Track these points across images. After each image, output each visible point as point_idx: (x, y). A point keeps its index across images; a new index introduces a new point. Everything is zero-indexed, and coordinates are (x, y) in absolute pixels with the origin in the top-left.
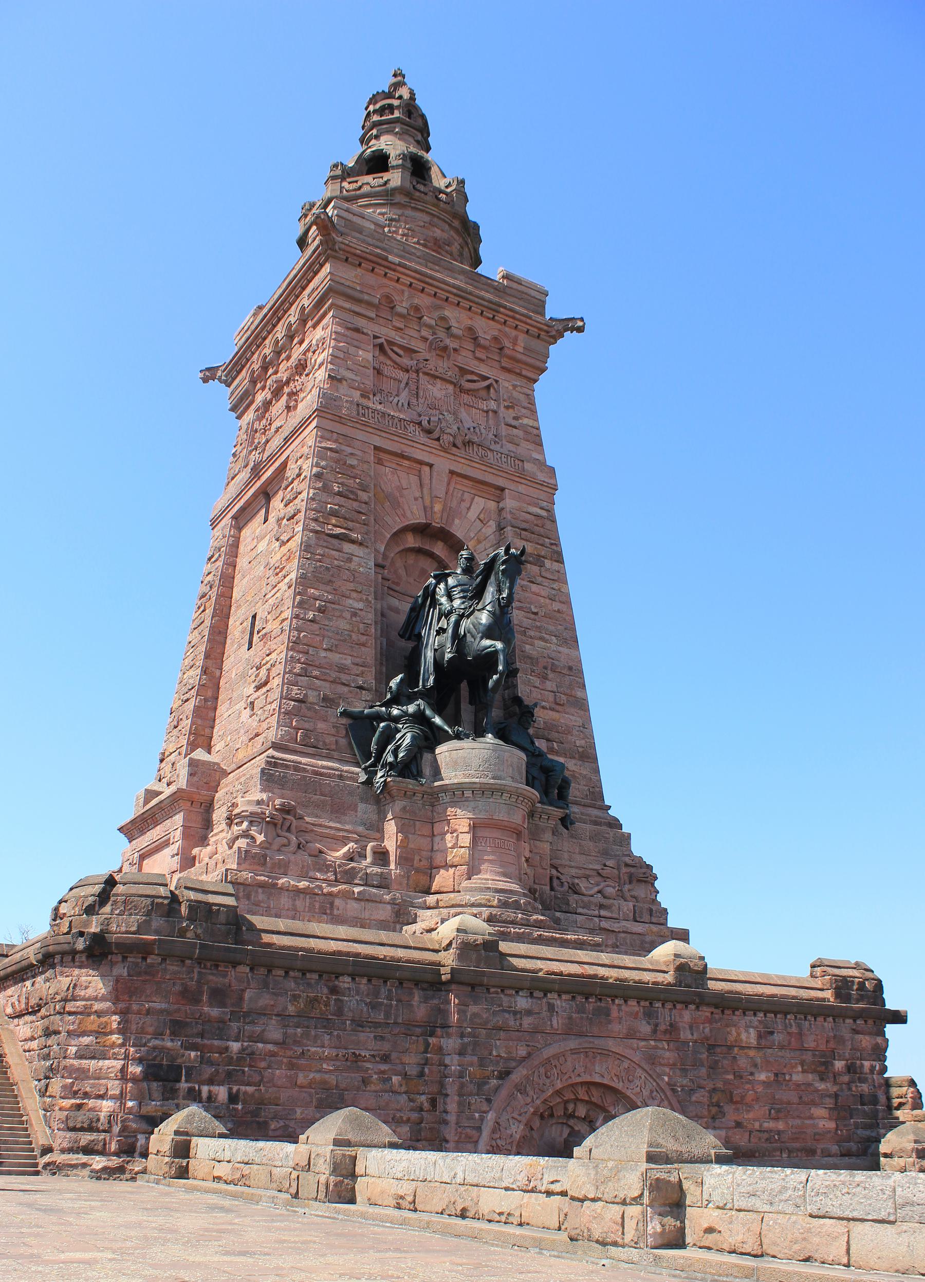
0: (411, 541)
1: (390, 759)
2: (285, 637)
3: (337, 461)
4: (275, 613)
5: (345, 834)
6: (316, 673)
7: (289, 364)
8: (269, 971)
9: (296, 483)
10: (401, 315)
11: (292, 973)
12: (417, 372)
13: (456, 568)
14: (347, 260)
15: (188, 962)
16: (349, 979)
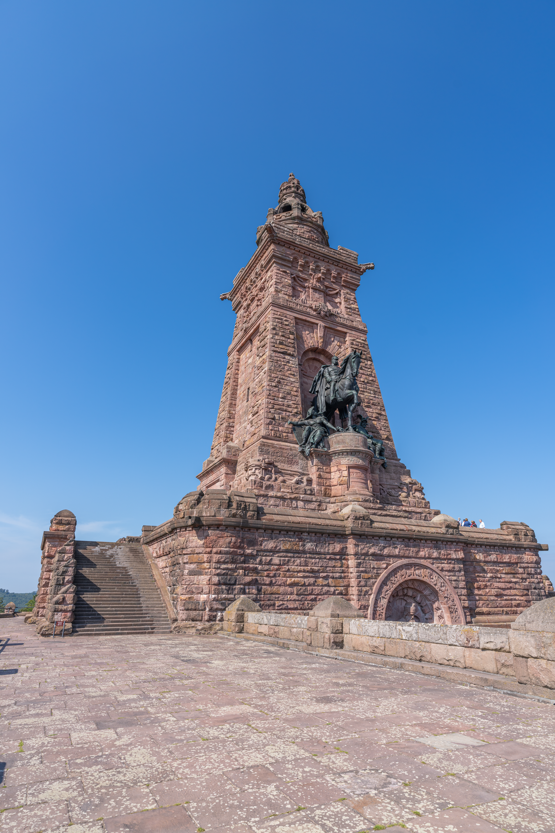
0: (311, 355)
1: (312, 441)
2: (264, 393)
3: (281, 323)
4: (259, 385)
5: (294, 473)
7: (257, 288)
8: (272, 531)
9: (264, 333)
11: (282, 532)
12: (309, 288)
13: (331, 363)
14: (279, 244)
15: (237, 529)
16: (306, 534)
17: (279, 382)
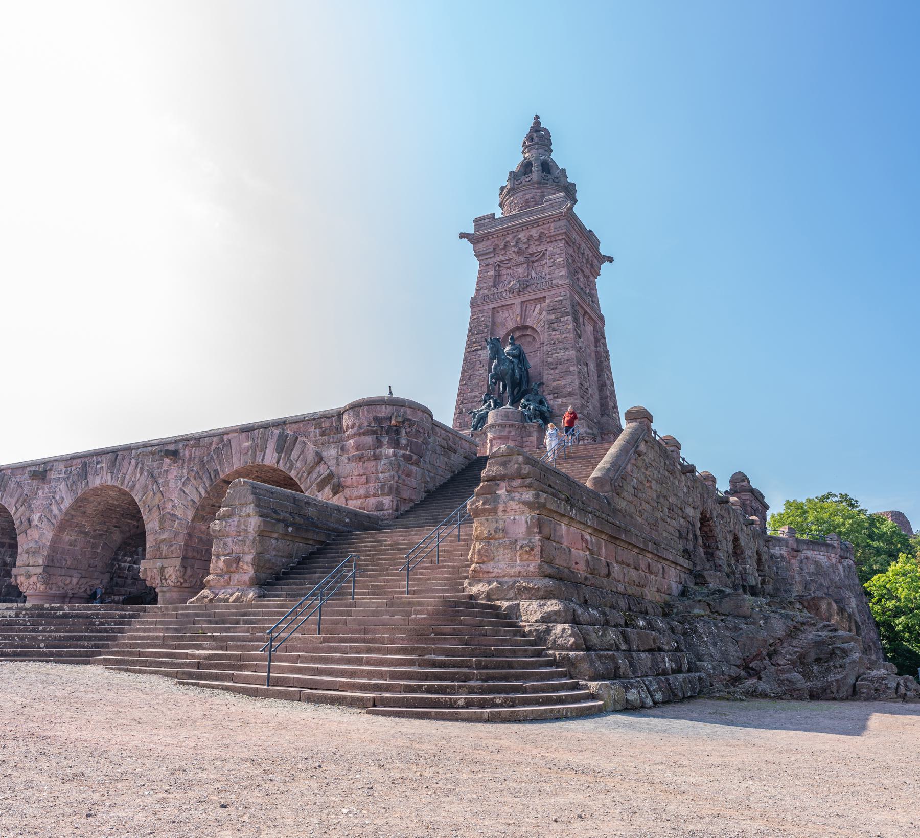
6: (466, 401)
10: (501, 249)
17: (469, 379)
